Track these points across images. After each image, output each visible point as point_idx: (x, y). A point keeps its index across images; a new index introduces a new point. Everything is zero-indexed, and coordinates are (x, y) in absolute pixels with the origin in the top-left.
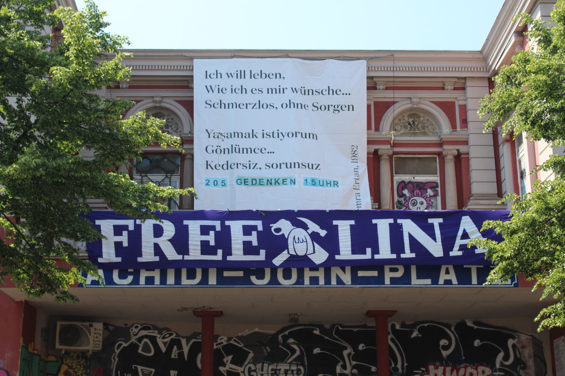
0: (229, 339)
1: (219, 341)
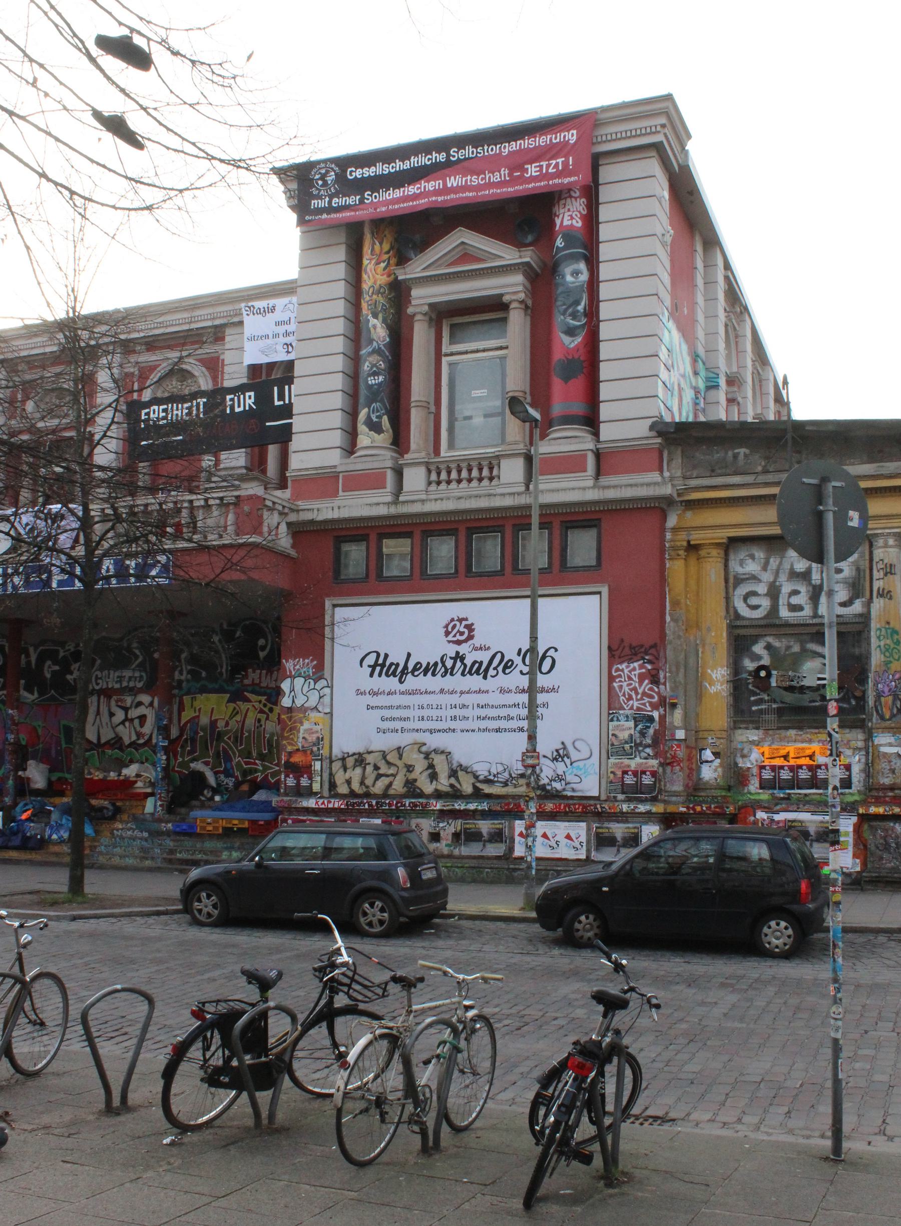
1: (67, 648)
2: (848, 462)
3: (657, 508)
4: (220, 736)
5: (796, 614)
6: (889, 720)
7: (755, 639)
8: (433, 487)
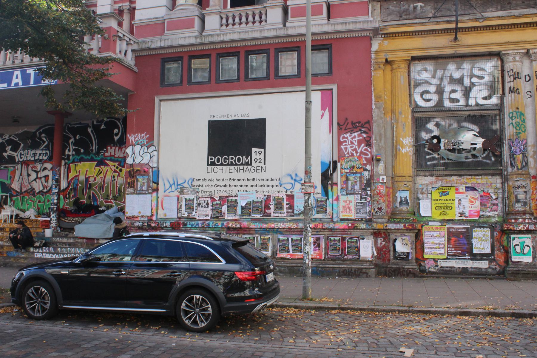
0: (10, 136)
1: (4, 137)
2: (488, 10)
3: (365, 38)
4: (91, 186)
5: (455, 104)
6: (521, 169)
7: (428, 120)
8: (224, 27)
